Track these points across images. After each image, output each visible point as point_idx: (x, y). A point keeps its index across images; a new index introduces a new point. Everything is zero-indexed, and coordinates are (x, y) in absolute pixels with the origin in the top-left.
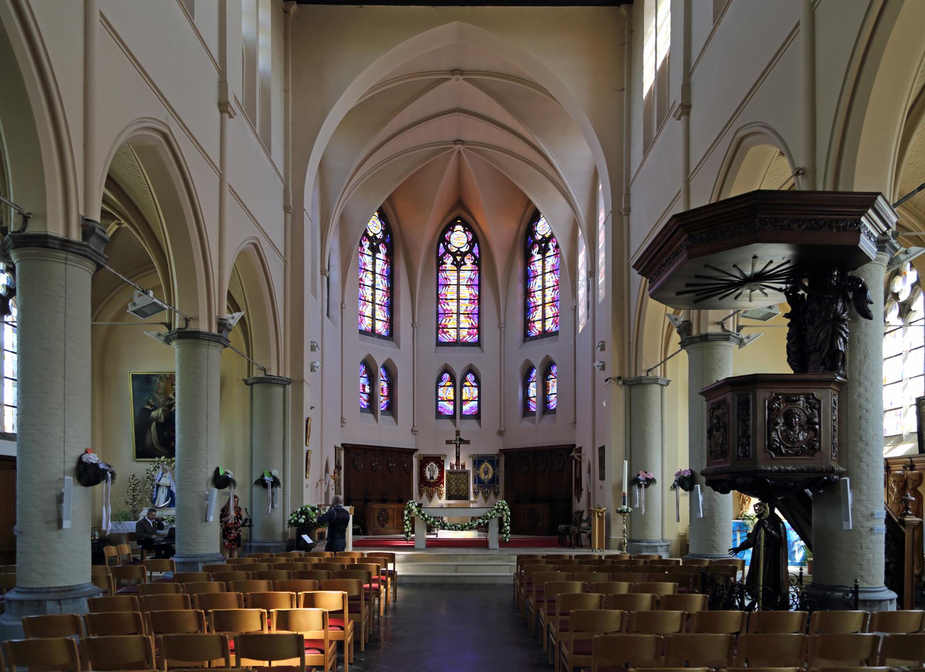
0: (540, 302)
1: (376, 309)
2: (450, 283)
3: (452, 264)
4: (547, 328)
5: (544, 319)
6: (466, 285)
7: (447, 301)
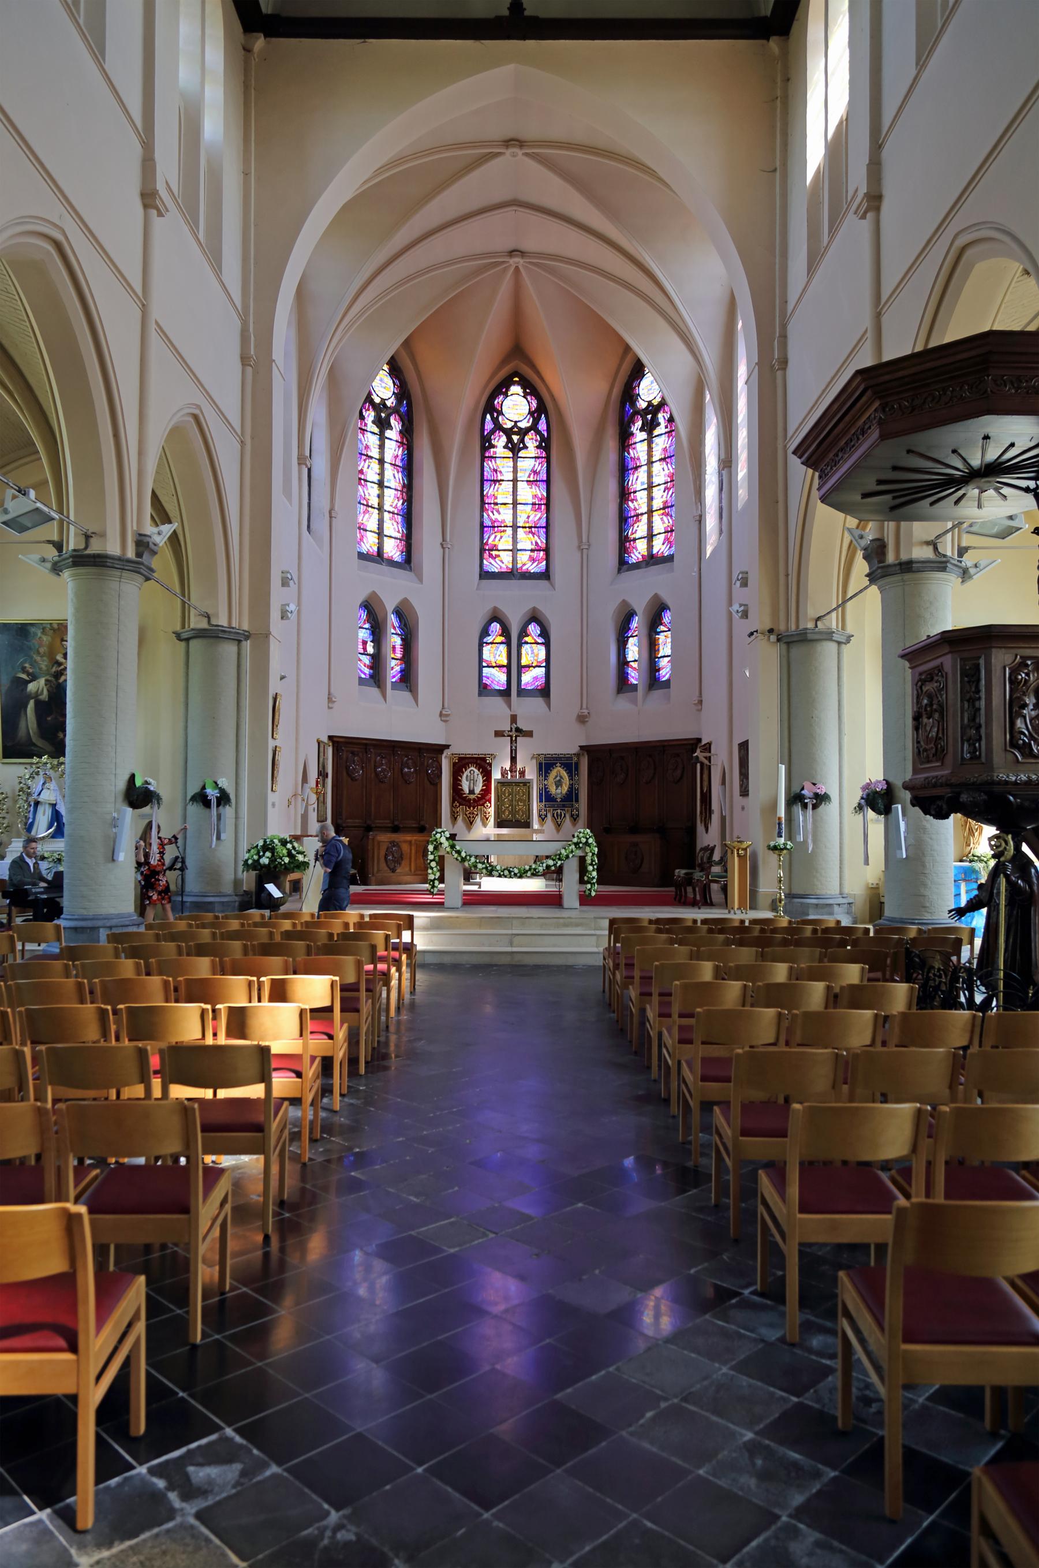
0: (644, 509)
1: (385, 519)
2: (502, 478)
3: (504, 447)
4: (655, 551)
5: (650, 537)
6: (527, 481)
7: (496, 507)
